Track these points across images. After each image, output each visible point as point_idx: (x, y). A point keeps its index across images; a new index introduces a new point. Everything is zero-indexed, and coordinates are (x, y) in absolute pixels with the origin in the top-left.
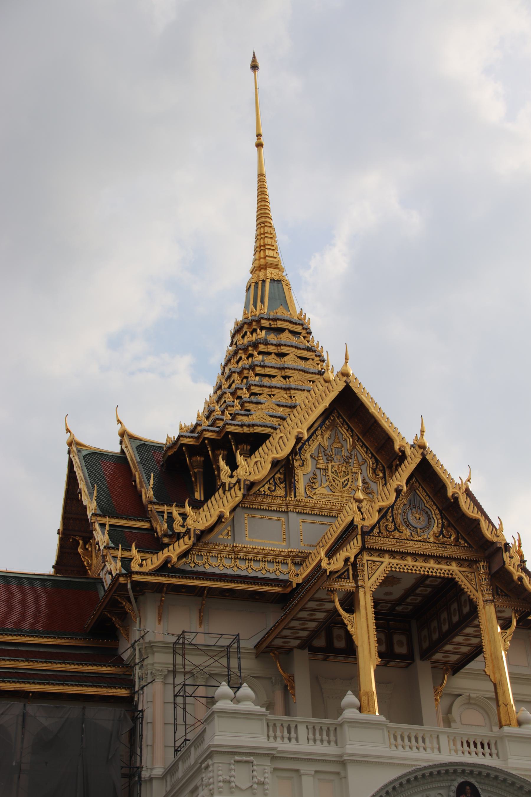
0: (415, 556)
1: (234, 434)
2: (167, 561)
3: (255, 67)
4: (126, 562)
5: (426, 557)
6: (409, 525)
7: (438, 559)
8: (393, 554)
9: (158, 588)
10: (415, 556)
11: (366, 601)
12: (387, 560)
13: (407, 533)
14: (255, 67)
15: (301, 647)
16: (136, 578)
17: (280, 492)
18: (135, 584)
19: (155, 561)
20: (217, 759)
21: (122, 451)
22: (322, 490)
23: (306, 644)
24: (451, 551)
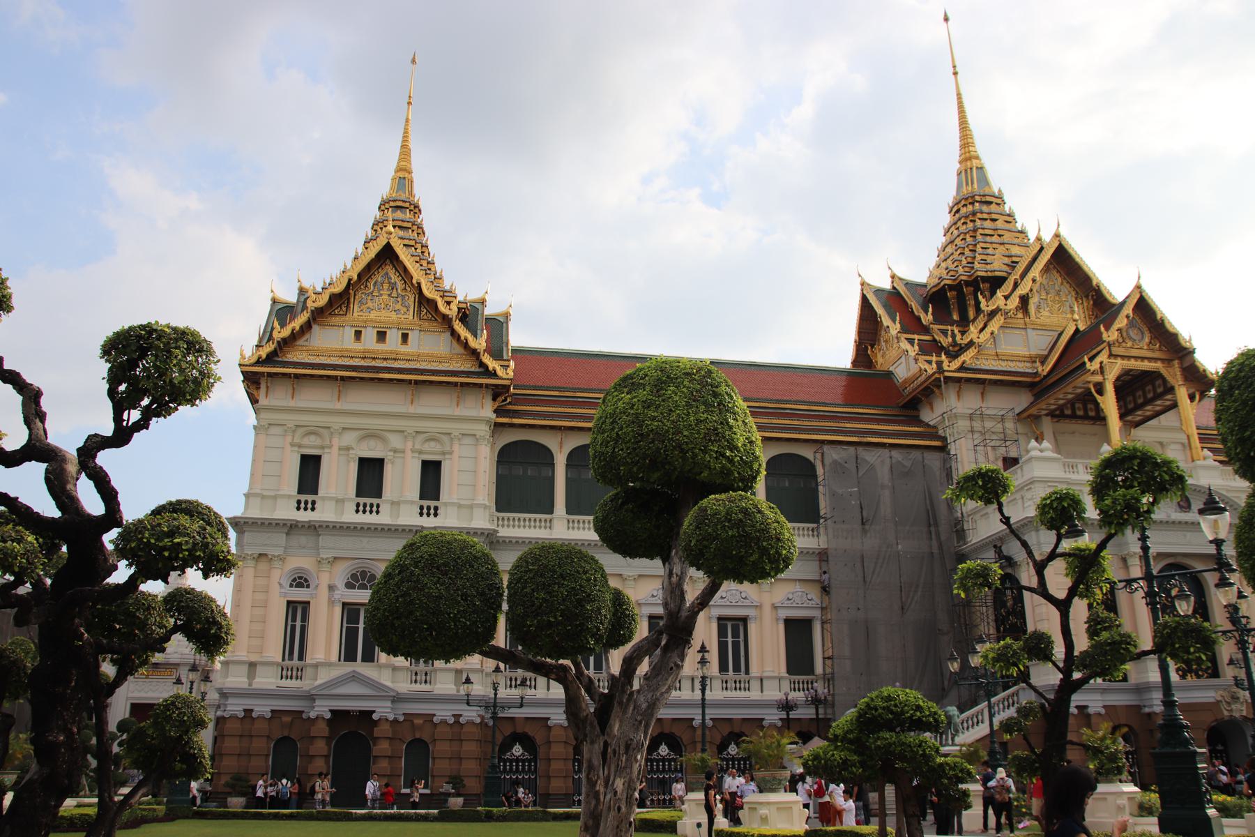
0: (1136, 358)
1: (982, 277)
2: (964, 362)
3: (946, 19)
4: (939, 364)
5: (1143, 359)
6: (1130, 338)
7: (1150, 359)
8: (1123, 357)
9: (959, 380)
10: (1136, 358)
11: (1110, 389)
12: (1119, 361)
13: (1129, 344)
14: (946, 19)
15: (1047, 415)
16: (947, 374)
17: (1020, 315)
18: (945, 378)
19: (956, 364)
20: (1037, 485)
21: (894, 288)
22: (1047, 314)
23: (1051, 414)
24: (1157, 355)
